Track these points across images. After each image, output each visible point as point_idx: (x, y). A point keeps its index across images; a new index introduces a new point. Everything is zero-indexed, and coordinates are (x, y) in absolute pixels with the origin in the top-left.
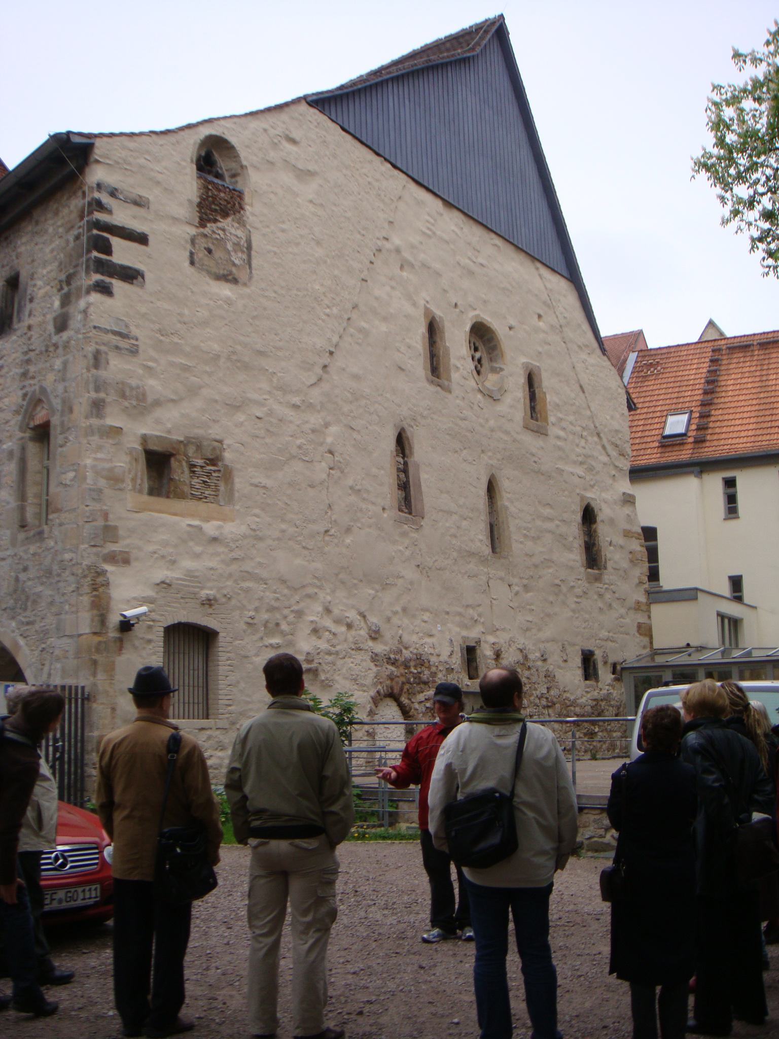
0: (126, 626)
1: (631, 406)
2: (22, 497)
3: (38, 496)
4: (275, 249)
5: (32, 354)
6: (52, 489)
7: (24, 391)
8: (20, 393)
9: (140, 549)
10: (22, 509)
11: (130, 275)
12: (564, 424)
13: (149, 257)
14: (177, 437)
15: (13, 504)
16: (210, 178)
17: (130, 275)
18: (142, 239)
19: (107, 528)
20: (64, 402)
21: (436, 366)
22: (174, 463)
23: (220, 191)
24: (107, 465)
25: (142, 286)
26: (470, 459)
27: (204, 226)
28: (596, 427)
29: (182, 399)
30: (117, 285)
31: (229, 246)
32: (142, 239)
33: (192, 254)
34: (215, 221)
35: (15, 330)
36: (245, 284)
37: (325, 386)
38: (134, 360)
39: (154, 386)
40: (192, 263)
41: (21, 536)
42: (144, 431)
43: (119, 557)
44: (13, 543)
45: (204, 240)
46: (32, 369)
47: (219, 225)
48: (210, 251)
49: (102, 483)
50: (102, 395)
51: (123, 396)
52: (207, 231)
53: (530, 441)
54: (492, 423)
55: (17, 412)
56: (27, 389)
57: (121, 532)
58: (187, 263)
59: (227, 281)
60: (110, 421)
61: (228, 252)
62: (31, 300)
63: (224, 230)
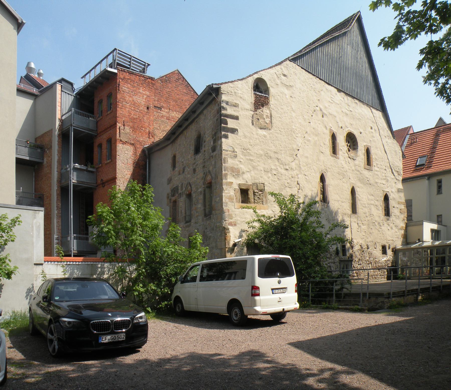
1: (404, 156)
4: (280, 116)
11: (233, 131)
12: (379, 166)
13: (239, 124)
14: (250, 183)
16: (258, 93)
17: (233, 131)
18: (236, 118)
19: (229, 215)
21: (334, 151)
22: (249, 192)
23: (261, 98)
24: (228, 195)
25: (237, 134)
26: (345, 182)
27: (256, 111)
28: (390, 166)
29: (251, 171)
30: (230, 135)
31: (265, 117)
32: (236, 118)
33: (252, 121)
34: (260, 108)
36: (270, 129)
37: (297, 162)
38: (236, 159)
39: (243, 167)
40: (253, 124)
43: (233, 224)
45: (256, 116)
47: (261, 110)
48: (258, 119)
49: (227, 200)
50: (226, 172)
51: (233, 172)
52: (258, 112)
53: (366, 173)
54: (353, 168)
57: (234, 216)
58: (251, 124)
59: (264, 129)
61: (264, 119)
63: (263, 111)
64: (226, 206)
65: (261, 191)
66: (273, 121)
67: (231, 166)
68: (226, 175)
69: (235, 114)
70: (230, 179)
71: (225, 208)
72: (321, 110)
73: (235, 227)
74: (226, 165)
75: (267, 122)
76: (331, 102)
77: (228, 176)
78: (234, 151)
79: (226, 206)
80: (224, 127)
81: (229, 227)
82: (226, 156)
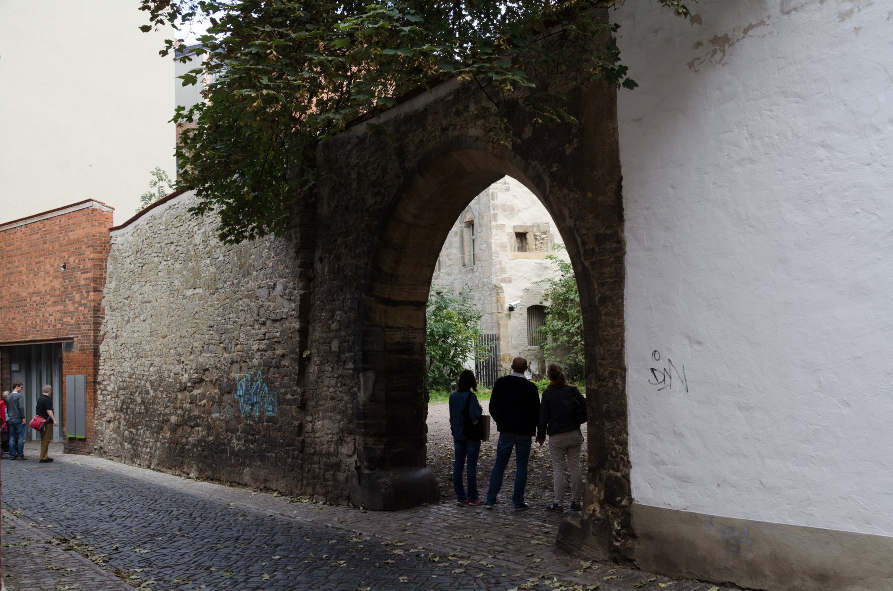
0: (511, 309)
2: (463, 253)
3: (469, 251)
6: (476, 251)
10: (463, 258)
14: (529, 224)
15: (459, 255)
19: (501, 268)
20: (479, 214)
22: (528, 236)
41: (464, 270)
44: (460, 272)
49: (498, 249)
60: (499, 222)
64: (497, 257)
68: (495, 216)
70: (501, 220)
71: (495, 259)
73: (511, 285)
74: (495, 202)
79: (497, 257)
81: (502, 285)
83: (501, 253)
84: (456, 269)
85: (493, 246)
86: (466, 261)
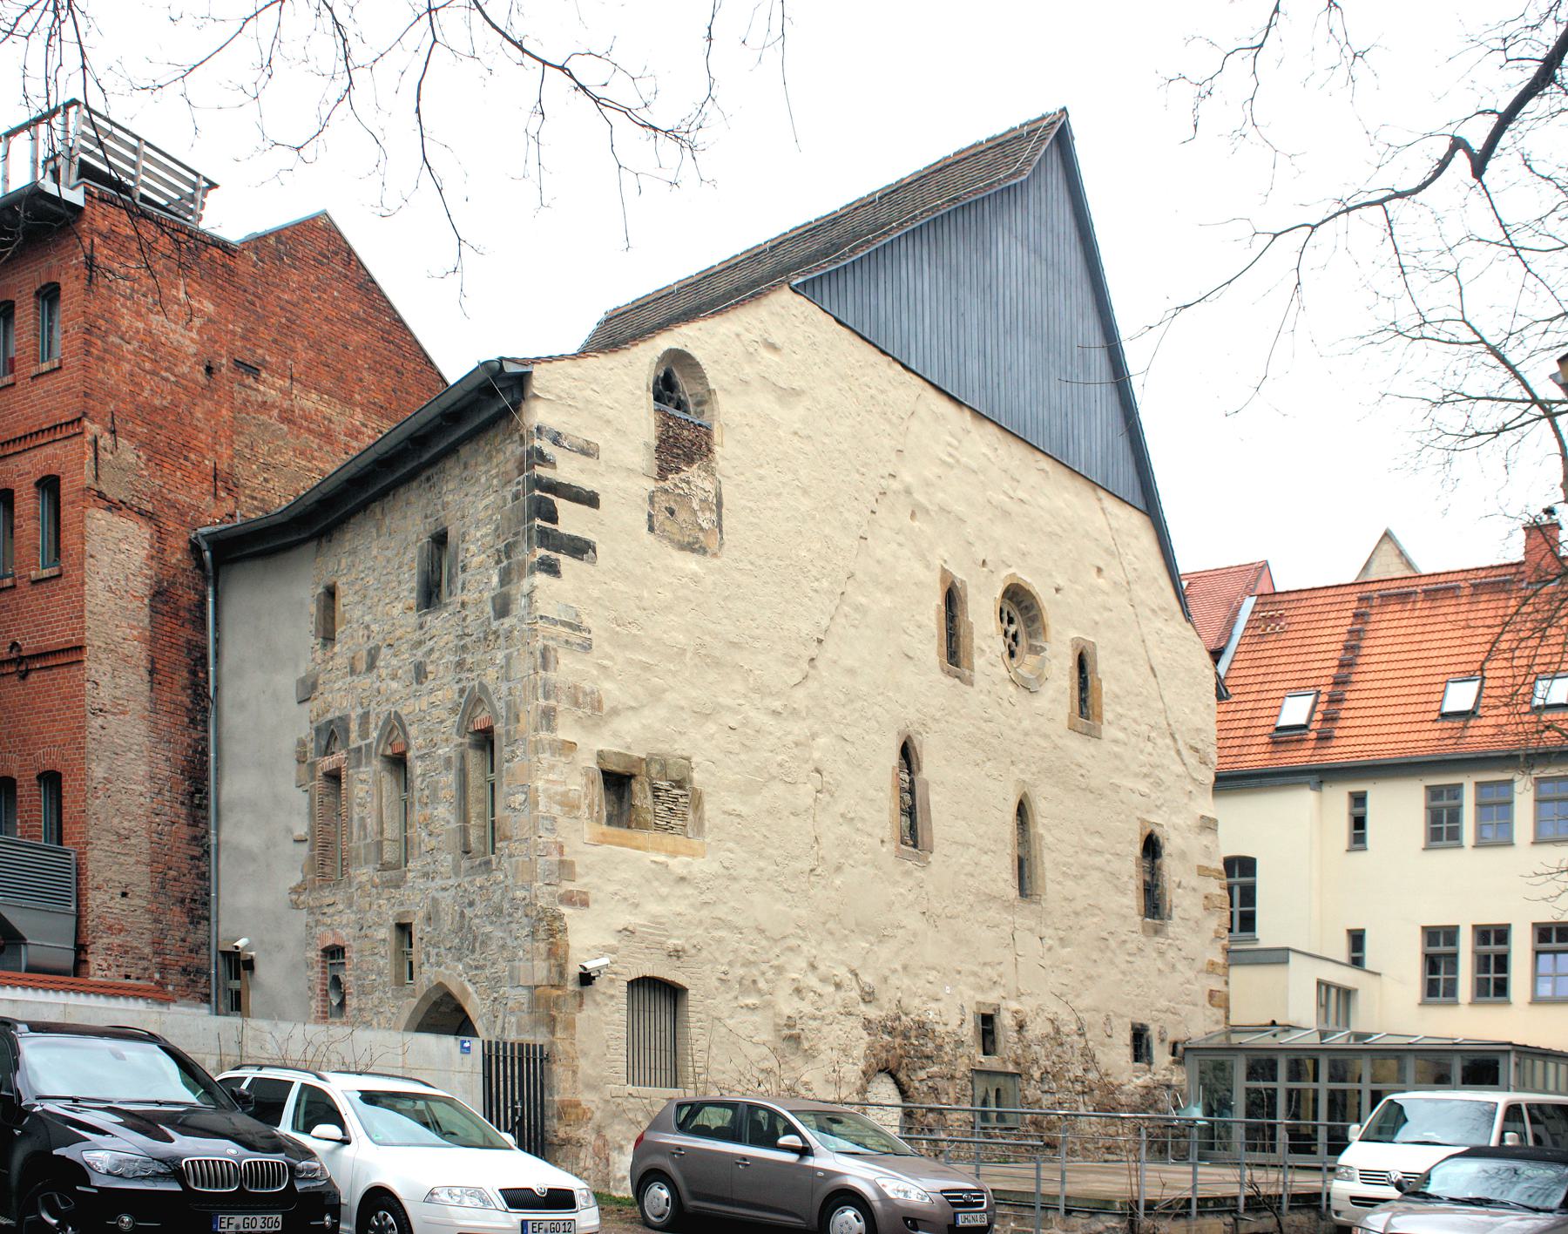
3: (481, 816)
5: (468, 639)
7: (460, 685)
8: (456, 687)
9: (599, 889)
11: (580, 548)
17: (580, 548)
18: (591, 500)
22: (636, 786)
25: (593, 562)
32: (591, 500)
35: (446, 605)
38: (587, 657)
39: (611, 691)
42: (601, 747)
46: (469, 660)
55: (453, 710)
56: (464, 683)
62: (464, 569)
65: (679, 784)
66: (725, 523)
67: (571, 679)
69: (586, 483)
72: (908, 492)
75: (704, 525)
76: (944, 462)
77: (560, 720)
78: (576, 628)
80: (543, 533)
82: (551, 643)
83: (563, 821)
84: (446, 860)
85: (542, 800)
86: (472, 839)
